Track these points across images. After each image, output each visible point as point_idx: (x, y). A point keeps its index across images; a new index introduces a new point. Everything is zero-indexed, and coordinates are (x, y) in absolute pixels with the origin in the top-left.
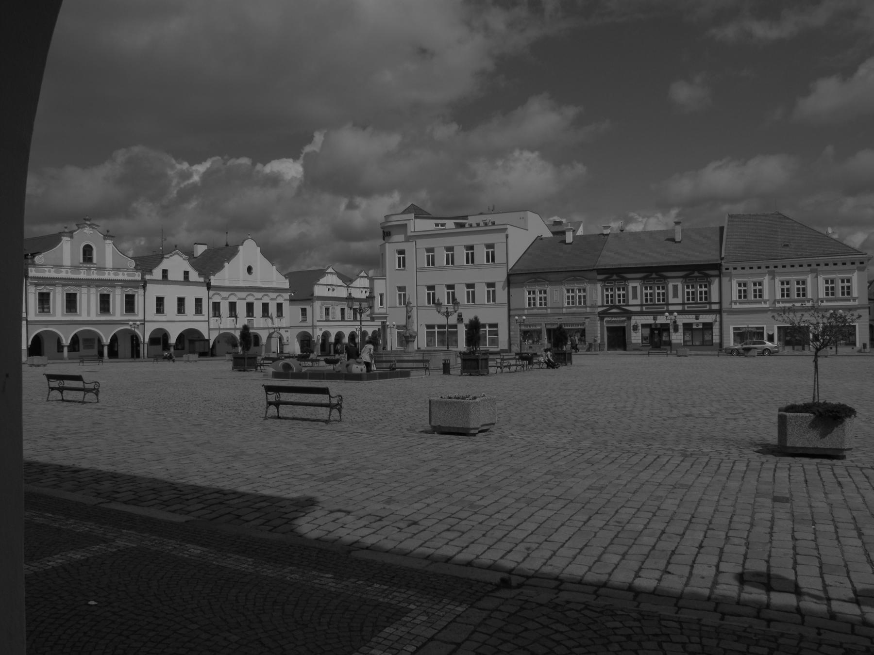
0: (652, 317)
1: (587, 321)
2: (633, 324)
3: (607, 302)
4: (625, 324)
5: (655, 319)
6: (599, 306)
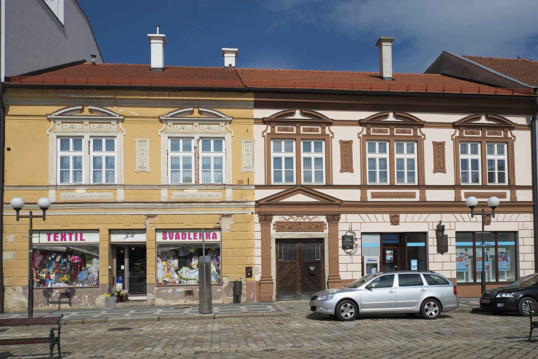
0: (387, 217)
1: (226, 224)
2: (344, 233)
3: (278, 178)
4: (324, 234)
5: (395, 221)
6: (258, 187)
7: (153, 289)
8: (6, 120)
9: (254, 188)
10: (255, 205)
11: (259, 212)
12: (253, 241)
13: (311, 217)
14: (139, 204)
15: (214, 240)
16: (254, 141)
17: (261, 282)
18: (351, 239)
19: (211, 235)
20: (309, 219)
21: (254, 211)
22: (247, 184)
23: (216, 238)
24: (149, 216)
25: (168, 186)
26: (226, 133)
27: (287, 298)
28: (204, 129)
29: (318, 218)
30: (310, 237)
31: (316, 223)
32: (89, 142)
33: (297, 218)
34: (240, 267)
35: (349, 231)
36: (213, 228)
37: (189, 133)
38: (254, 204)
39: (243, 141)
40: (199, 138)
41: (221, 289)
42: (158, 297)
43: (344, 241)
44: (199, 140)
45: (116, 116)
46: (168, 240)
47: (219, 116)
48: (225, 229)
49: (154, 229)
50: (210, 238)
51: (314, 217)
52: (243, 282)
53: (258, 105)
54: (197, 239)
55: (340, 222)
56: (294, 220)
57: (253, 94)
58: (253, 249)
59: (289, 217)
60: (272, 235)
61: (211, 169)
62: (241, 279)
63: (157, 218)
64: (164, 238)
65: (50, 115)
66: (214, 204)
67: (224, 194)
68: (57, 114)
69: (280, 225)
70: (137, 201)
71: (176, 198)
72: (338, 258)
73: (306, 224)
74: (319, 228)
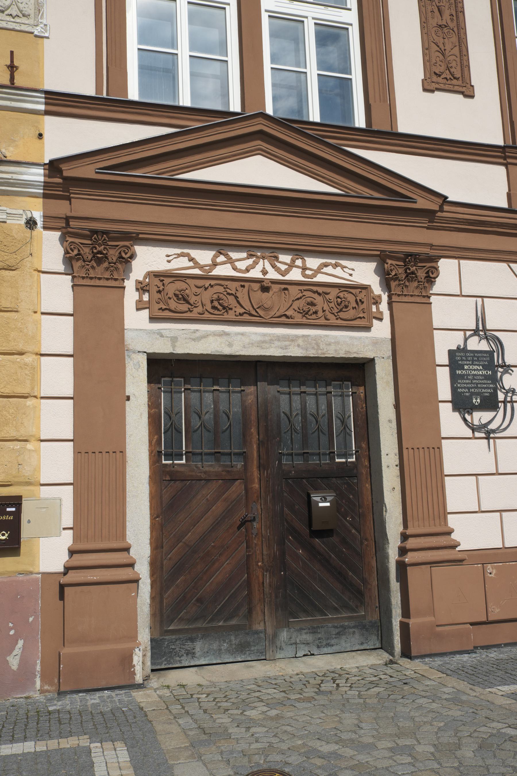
9: (42, 107)
10: (46, 185)
11: (67, 219)
12: (28, 359)
13: (313, 263)
17: (73, 577)
18: (485, 368)
20: (304, 269)
21: (38, 216)
27: (205, 654)
29: (343, 267)
30: (312, 353)
31: (334, 292)
33: (250, 261)
35: (476, 332)
43: (459, 372)
51: (326, 265)
55: (436, 289)
56: (235, 269)
58: (29, 402)
59: (215, 257)
60: (128, 335)
69: (172, 289)
72: (440, 448)
73: (294, 291)
74: (350, 313)
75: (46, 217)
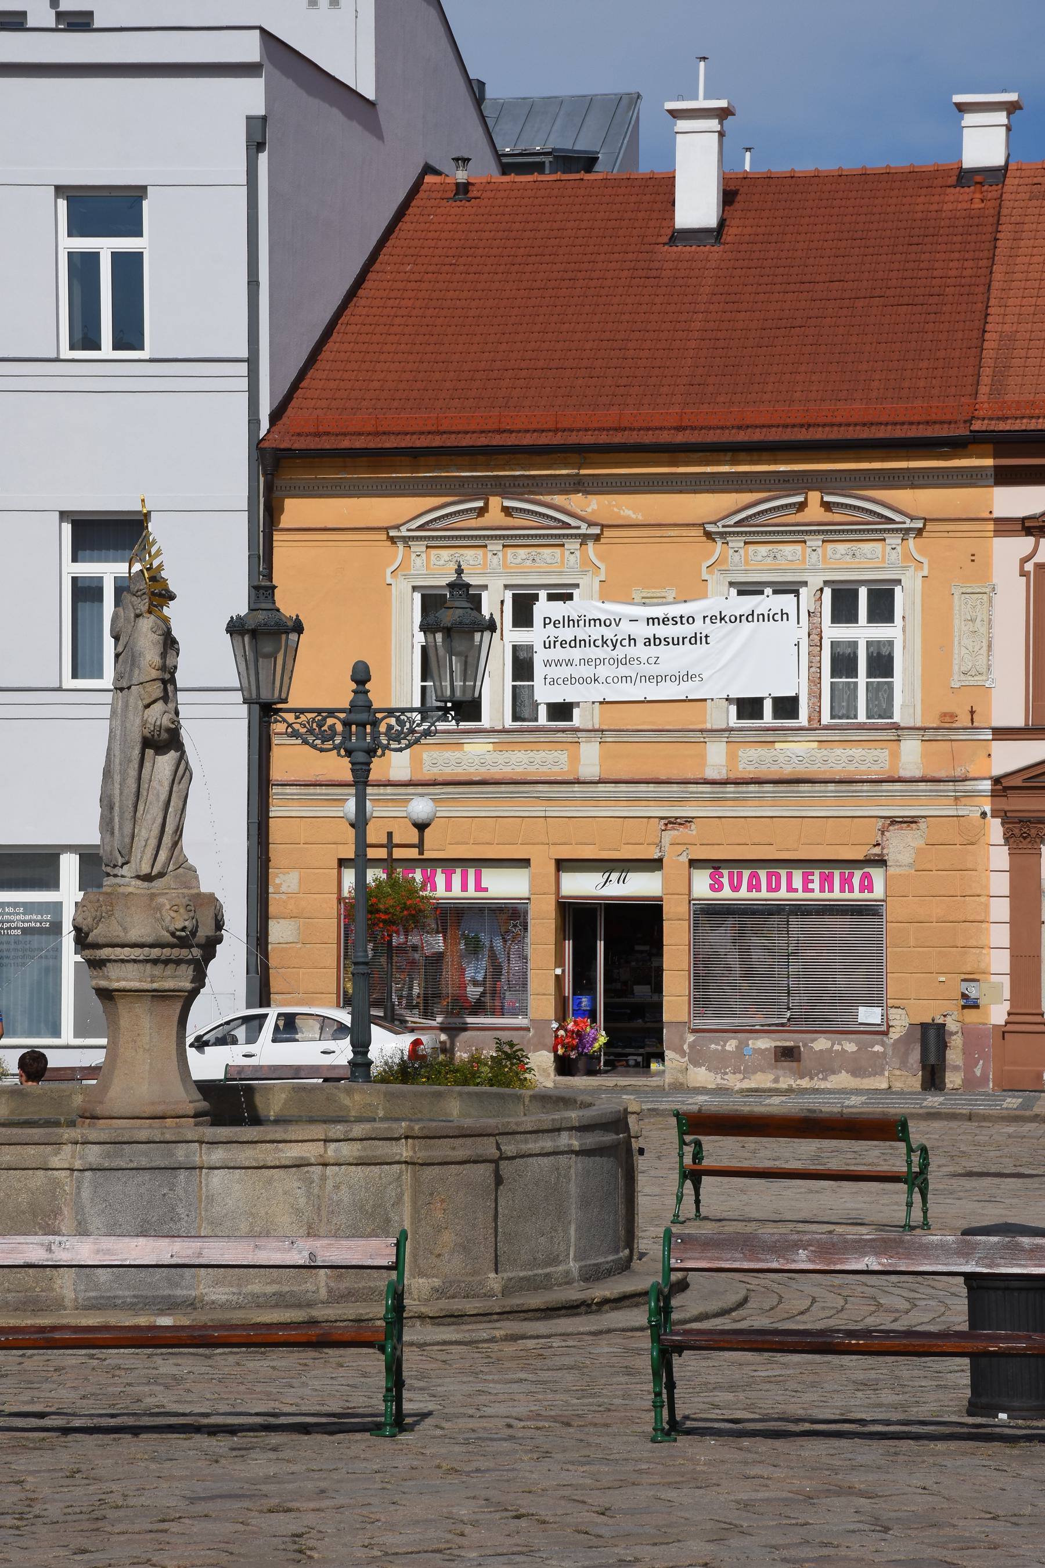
6: (1002, 733)
7: (683, 1040)
8: (275, 544)
9: (990, 737)
10: (992, 791)
11: (1005, 812)
12: (983, 899)
14: (642, 787)
15: (866, 895)
16: (994, 589)
17: (1010, 1028)
19: (856, 881)
21: (988, 809)
22: (970, 725)
23: (871, 890)
24: (671, 823)
25: (726, 734)
26: (905, 568)
28: (838, 556)
32: (502, 602)
34: (943, 979)
36: (862, 858)
37: (794, 571)
38: (990, 787)
39: (957, 592)
40: (821, 585)
41: (883, 1046)
42: (696, 1064)
44: (821, 590)
45: (579, 528)
46: (727, 892)
47: (886, 518)
48: (897, 861)
49: (684, 859)
50: (851, 890)
52: (952, 1026)
53: (1005, 477)
54: (812, 890)
57: (990, 448)
58: (984, 925)
61: (893, 677)
62: (945, 1016)
63: (693, 826)
64: (716, 887)
65: (397, 527)
66: (866, 787)
67: (895, 756)
68: (414, 527)
70: (637, 777)
71: (751, 768)
75: (992, 810)
